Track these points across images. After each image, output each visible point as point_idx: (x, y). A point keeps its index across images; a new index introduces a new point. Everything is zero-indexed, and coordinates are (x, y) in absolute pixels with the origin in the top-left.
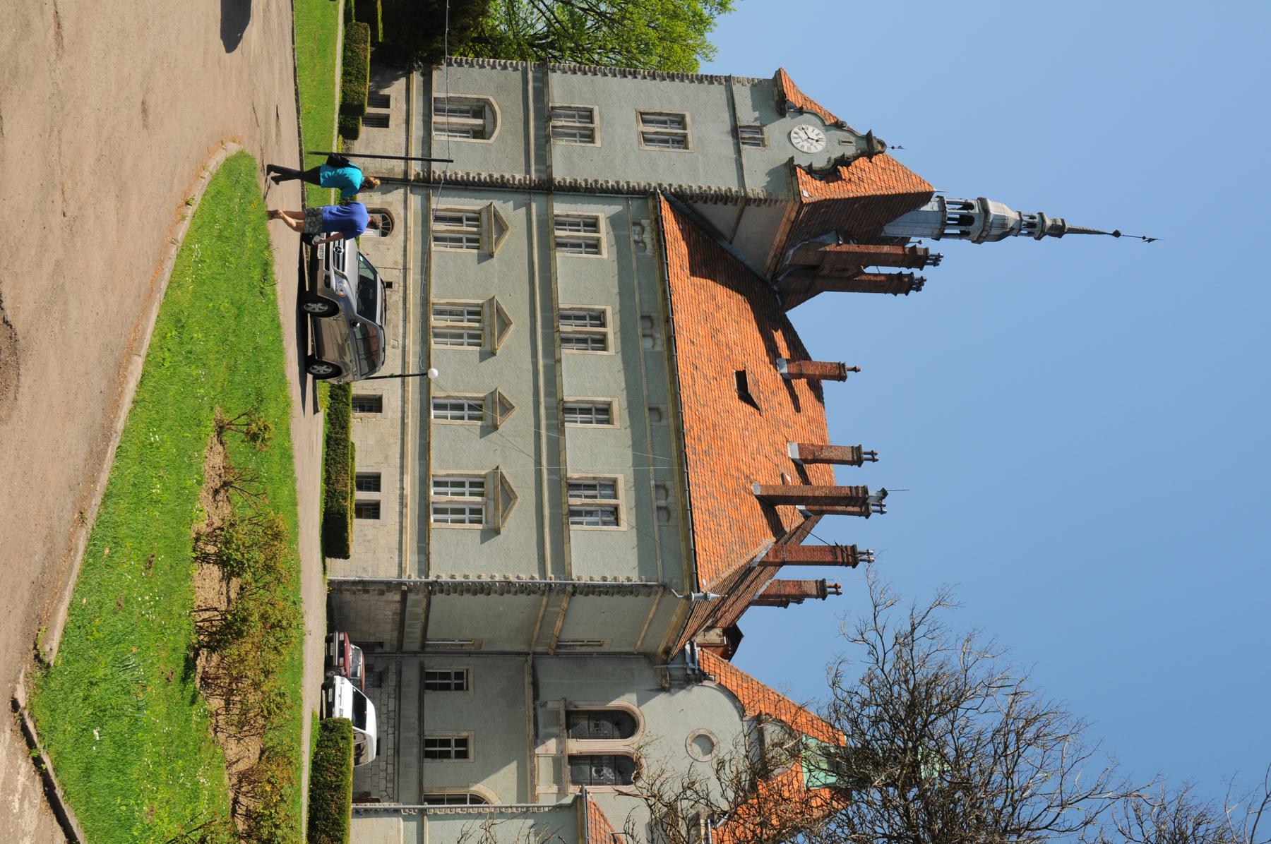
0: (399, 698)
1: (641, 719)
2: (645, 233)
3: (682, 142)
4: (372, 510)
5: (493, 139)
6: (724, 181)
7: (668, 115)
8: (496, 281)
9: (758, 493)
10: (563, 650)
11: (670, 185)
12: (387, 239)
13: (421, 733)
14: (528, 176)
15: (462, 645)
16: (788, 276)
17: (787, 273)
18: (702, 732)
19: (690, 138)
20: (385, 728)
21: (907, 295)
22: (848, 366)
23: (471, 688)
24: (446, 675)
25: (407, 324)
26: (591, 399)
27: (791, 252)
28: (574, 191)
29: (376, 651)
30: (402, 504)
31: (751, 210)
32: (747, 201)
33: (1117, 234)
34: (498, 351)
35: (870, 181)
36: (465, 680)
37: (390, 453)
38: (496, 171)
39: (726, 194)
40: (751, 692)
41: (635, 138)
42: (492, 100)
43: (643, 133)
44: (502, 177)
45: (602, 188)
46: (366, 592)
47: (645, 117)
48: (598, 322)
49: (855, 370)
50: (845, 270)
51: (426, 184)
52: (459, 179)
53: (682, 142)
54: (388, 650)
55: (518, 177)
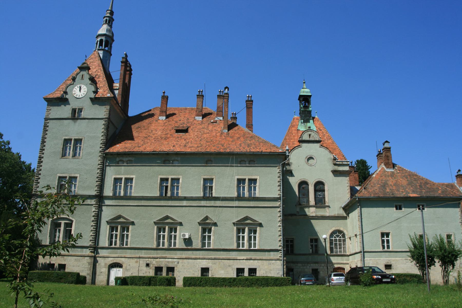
0: (297, 262)
1: (302, 180)
2: (123, 160)
3: (78, 141)
4: (253, 271)
5: (73, 219)
8: (145, 221)
9: (227, 131)
11: (101, 147)
18: (306, 160)
22: (163, 95)
23: (293, 237)
25: (167, 257)
28: (101, 187)
30: (250, 259)
35: (97, 72)
37: (228, 264)
38: (91, 219)
39: (106, 126)
41: (75, 160)
43: (72, 157)
44: (94, 216)
45: (101, 175)
47: (64, 155)
49: (164, 93)
51: (95, 248)
52: (94, 234)
53: (78, 141)
55: (94, 210)
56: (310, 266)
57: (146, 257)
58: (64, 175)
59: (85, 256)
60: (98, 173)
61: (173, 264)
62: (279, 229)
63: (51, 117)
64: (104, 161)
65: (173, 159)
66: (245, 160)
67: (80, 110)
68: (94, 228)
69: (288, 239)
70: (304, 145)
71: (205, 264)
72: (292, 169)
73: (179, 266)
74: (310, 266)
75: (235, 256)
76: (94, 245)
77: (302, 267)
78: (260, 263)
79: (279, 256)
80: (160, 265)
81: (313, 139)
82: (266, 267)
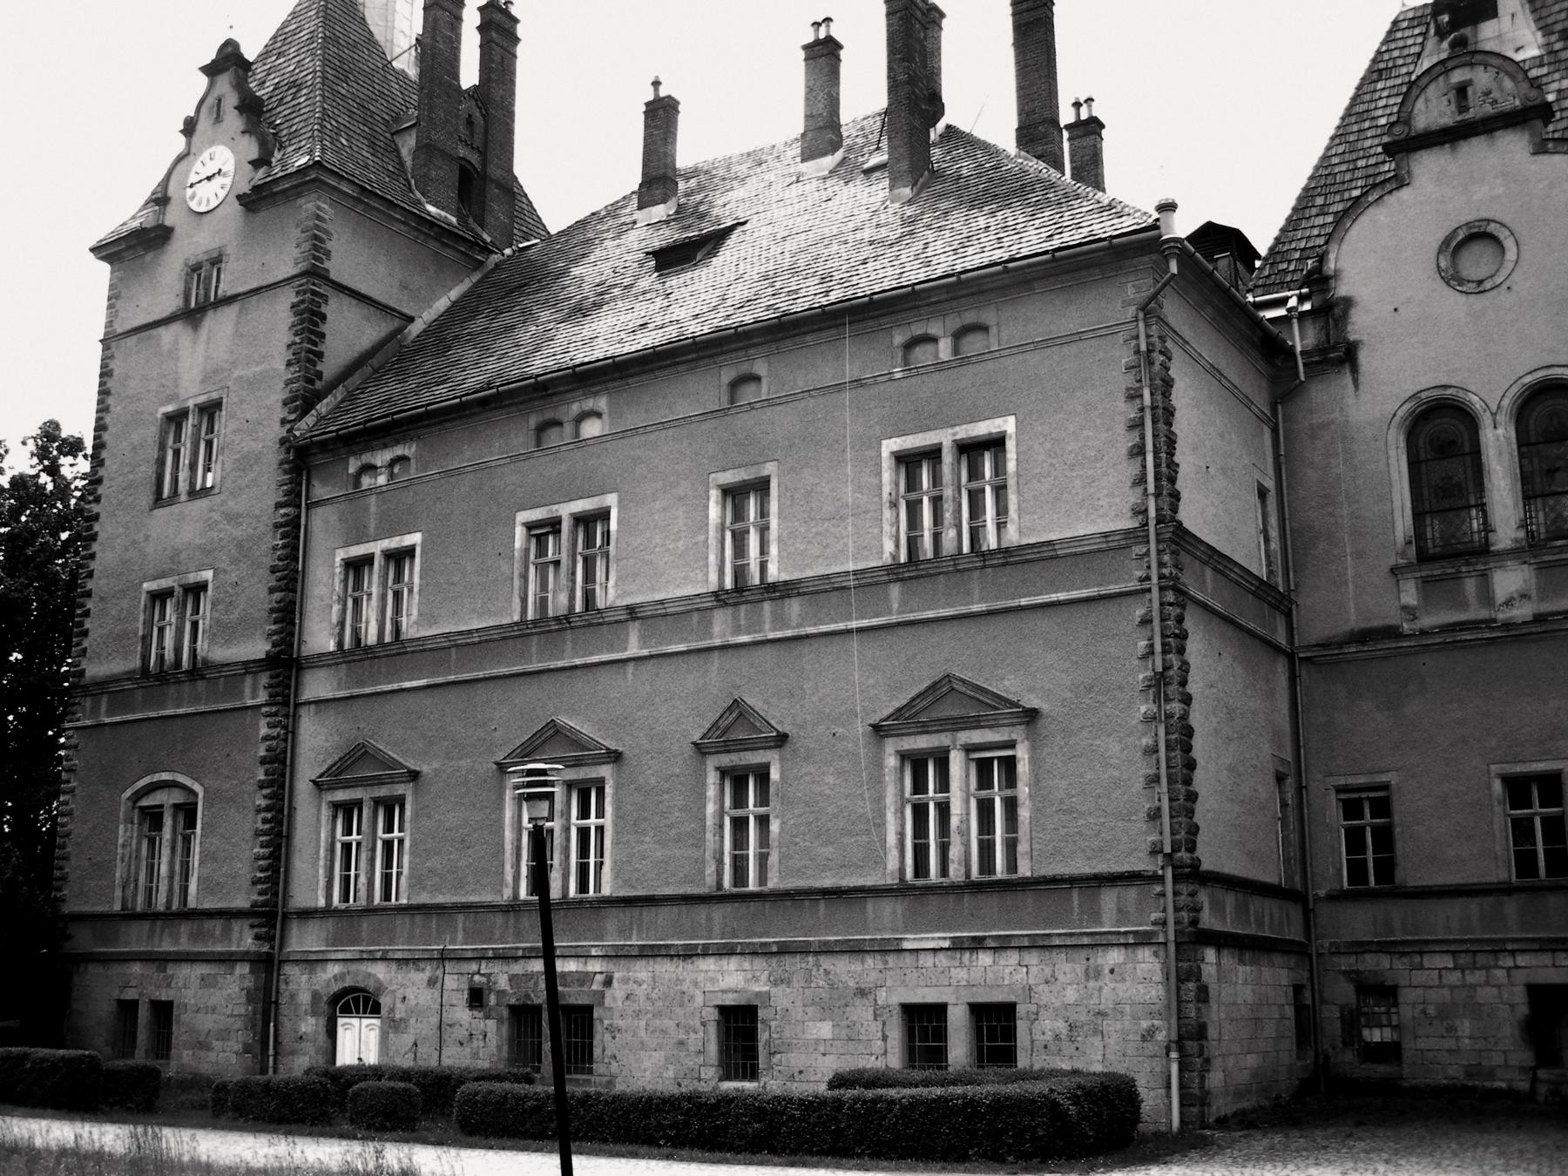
0: (1421, 947)
3: (210, 410)
5: (197, 787)
6: (277, 317)
7: (162, 447)
12: (385, 1001)
13: (1505, 890)
14: (264, 710)
16: (482, 226)
17: (479, 229)
19: (201, 399)
20: (1500, 974)
23: (1383, 778)
24: (1355, 840)
26: (713, 534)
27: (430, 208)
29: (1309, 1002)
30: (977, 945)
34: (613, 747)
36: (1364, 795)
37: (852, 984)
40: (1335, 188)
42: (128, 793)
44: (263, 761)
46: (1201, 1032)
48: (551, 538)
49: (656, 84)
50: (470, 122)
52: (266, 851)
53: (210, 410)
54: (1306, 975)
55: (264, 731)
56: (1509, 969)
57: (469, 955)
58: (164, 583)
59: (228, 960)
60: (275, 548)
61: (585, 989)
62: (1147, 741)
63: (119, 331)
65: (575, 408)
66: (934, 329)
67: (217, 261)
68: (265, 821)
69: (1355, 796)
70: (1427, 165)
72: (1352, 338)
73: (614, 999)
74: (1517, 967)
75: (894, 930)
76: (264, 904)
77: (1454, 978)
78: (1034, 970)
79: (1154, 916)
80: (527, 996)
82: (1071, 995)
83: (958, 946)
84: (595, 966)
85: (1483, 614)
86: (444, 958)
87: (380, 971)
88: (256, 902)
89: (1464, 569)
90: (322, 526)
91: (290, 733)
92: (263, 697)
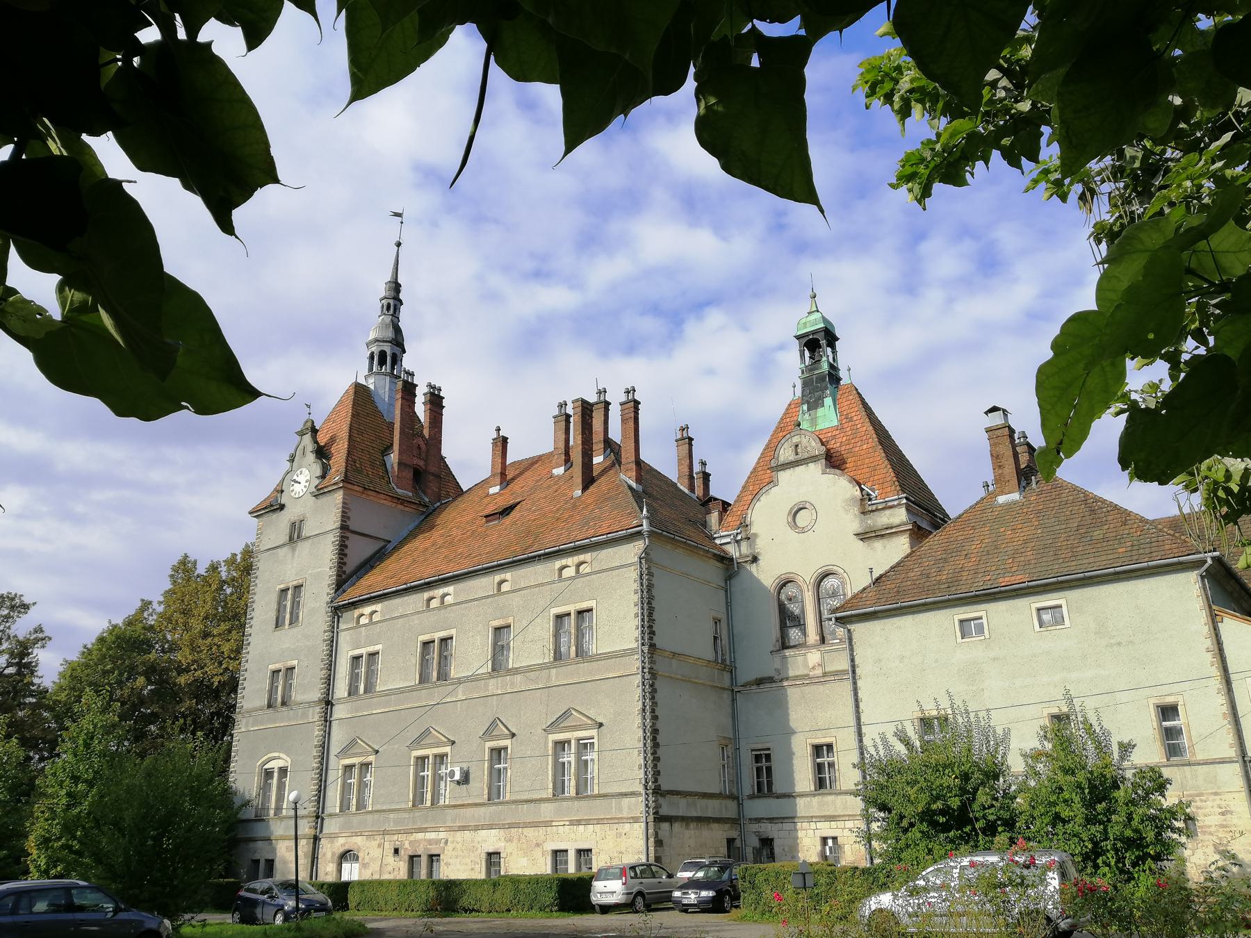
3: (298, 588)
9: (580, 491)
10: (728, 657)
12: (361, 855)
15: (728, 757)
21: (444, 398)
27: (398, 490)
28: (329, 681)
29: (739, 845)
30: (578, 822)
31: (353, 525)
32: (344, 527)
33: (399, 245)
36: (762, 752)
47: (278, 624)
49: (498, 430)
50: (419, 447)
53: (298, 588)
64: (334, 622)
69: (758, 753)
70: (784, 476)
71: (491, 840)
73: (448, 851)
74: (817, 829)
81: (806, 455)
83: (572, 823)
84: (442, 835)
85: (805, 672)
86: (385, 833)
87: (359, 841)
88: (310, 811)
89: (797, 653)
90: (344, 639)
91: (327, 734)
92: (316, 718)
